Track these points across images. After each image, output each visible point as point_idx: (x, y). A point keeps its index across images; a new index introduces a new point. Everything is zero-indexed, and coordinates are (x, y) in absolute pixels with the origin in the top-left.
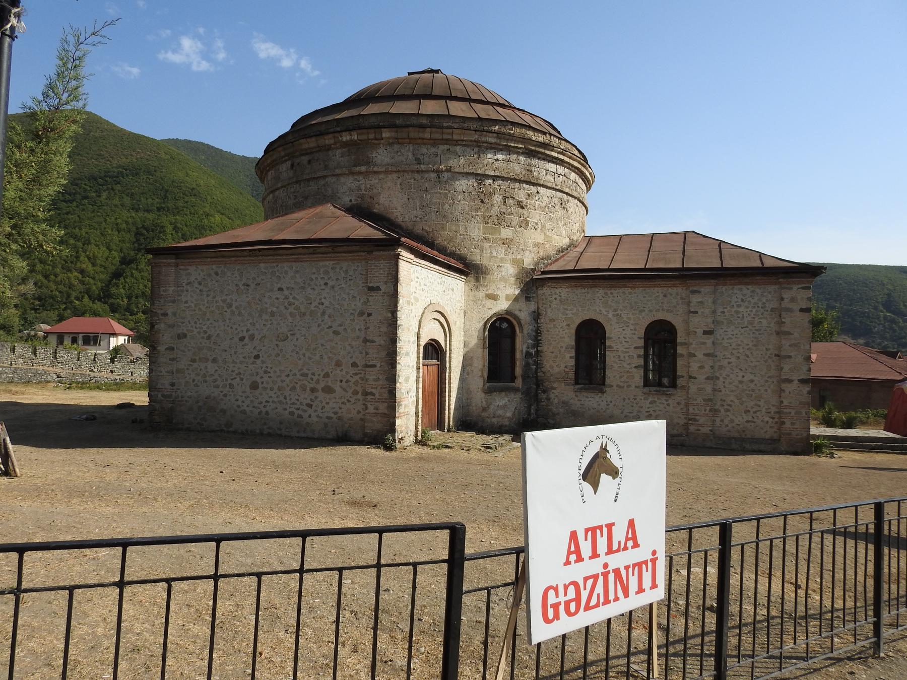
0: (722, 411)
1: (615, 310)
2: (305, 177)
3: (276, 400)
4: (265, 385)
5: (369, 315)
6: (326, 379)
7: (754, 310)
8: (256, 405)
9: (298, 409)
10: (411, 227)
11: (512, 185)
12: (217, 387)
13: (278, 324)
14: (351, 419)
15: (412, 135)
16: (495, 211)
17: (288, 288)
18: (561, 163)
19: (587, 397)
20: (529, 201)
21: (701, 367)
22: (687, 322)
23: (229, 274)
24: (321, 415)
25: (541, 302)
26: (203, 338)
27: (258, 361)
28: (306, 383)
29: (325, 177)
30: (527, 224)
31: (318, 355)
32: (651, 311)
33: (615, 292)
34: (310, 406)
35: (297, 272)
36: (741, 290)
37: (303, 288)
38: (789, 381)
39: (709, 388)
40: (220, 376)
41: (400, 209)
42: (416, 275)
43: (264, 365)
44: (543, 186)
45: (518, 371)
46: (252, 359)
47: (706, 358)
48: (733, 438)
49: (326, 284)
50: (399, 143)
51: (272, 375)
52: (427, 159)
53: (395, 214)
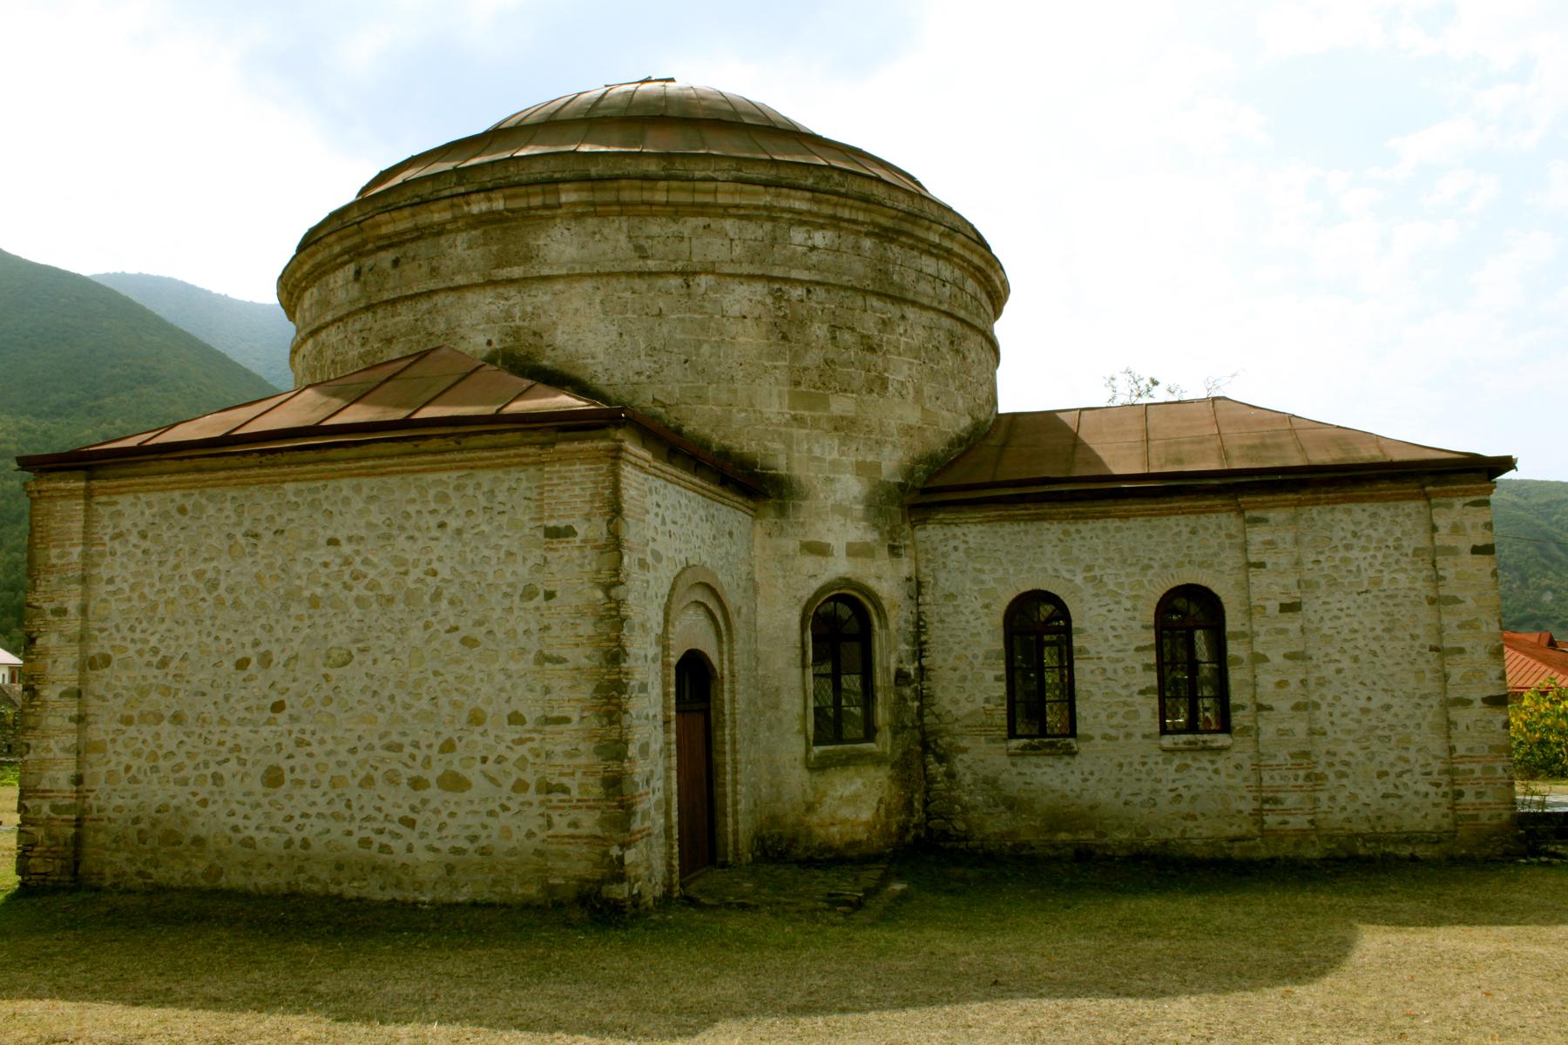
0: (1332, 777)
1: (1089, 568)
2: (386, 296)
3: (327, 812)
4: (298, 775)
5: (550, 595)
6: (447, 757)
7: (1379, 555)
8: (280, 824)
9: (381, 832)
10: (627, 398)
12: (184, 782)
13: (328, 625)
14: (512, 852)
15: (626, 196)
16: (813, 358)
17: (350, 539)
18: (947, 255)
19: (1037, 766)
21: (1282, 684)
22: (1246, 586)
23: (211, 510)
24: (437, 844)
25: (921, 556)
26: (149, 664)
27: (282, 717)
28: (399, 767)
29: (430, 293)
30: (884, 384)
31: (426, 698)
32: (1165, 566)
33: (1088, 528)
34: (409, 823)
35: (371, 499)
36: (1349, 512)
37: (388, 537)
38: (1465, 703)
39: (1300, 728)
40: (190, 755)
41: (601, 357)
42: (655, 498)
43: (296, 727)
44: (914, 303)
45: (882, 715)
46: (268, 714)
47: (1289, 663)
48: (1357, 835)
49: (442, 525)
50: (596, 214)
51: (315, 748)
52: (660, 247)
53: (590, 370)
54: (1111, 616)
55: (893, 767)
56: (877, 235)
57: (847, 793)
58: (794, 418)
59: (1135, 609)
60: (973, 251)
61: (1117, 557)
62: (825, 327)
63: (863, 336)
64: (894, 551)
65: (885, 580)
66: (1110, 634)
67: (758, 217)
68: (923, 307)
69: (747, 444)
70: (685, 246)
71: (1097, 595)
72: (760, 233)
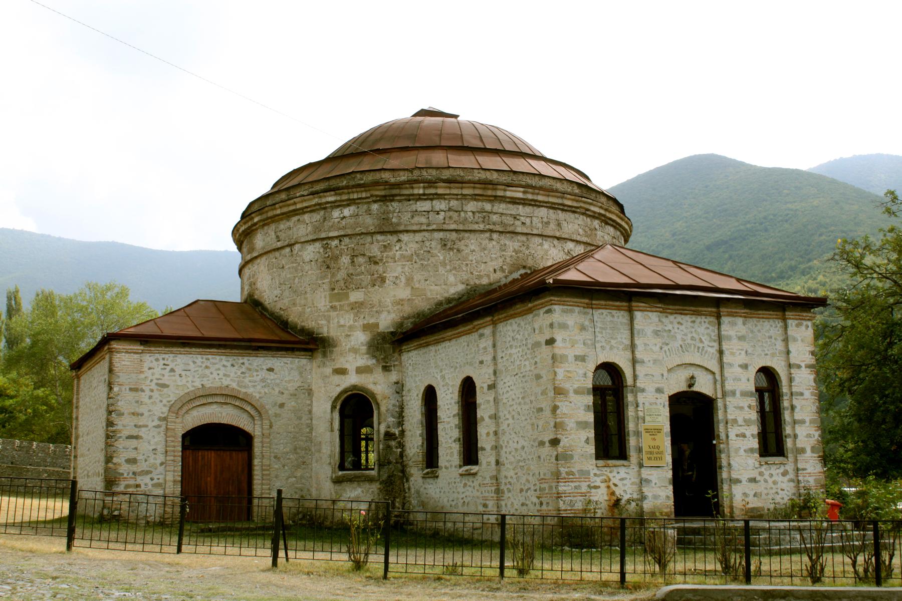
11: (361, 241)
16: (341, 275)
20: (385, 255)
30: (383, 280)
42: (162, 362)
44: (407, 231)
55: (381, 484)
56: (379, 201)
58: (332, 307)
63: (370, 258)
64: (386, 369)
65: (378, 385)
67: (317, 210)
68: (415, 231)
69: (310, 324)
72: (319, 217)
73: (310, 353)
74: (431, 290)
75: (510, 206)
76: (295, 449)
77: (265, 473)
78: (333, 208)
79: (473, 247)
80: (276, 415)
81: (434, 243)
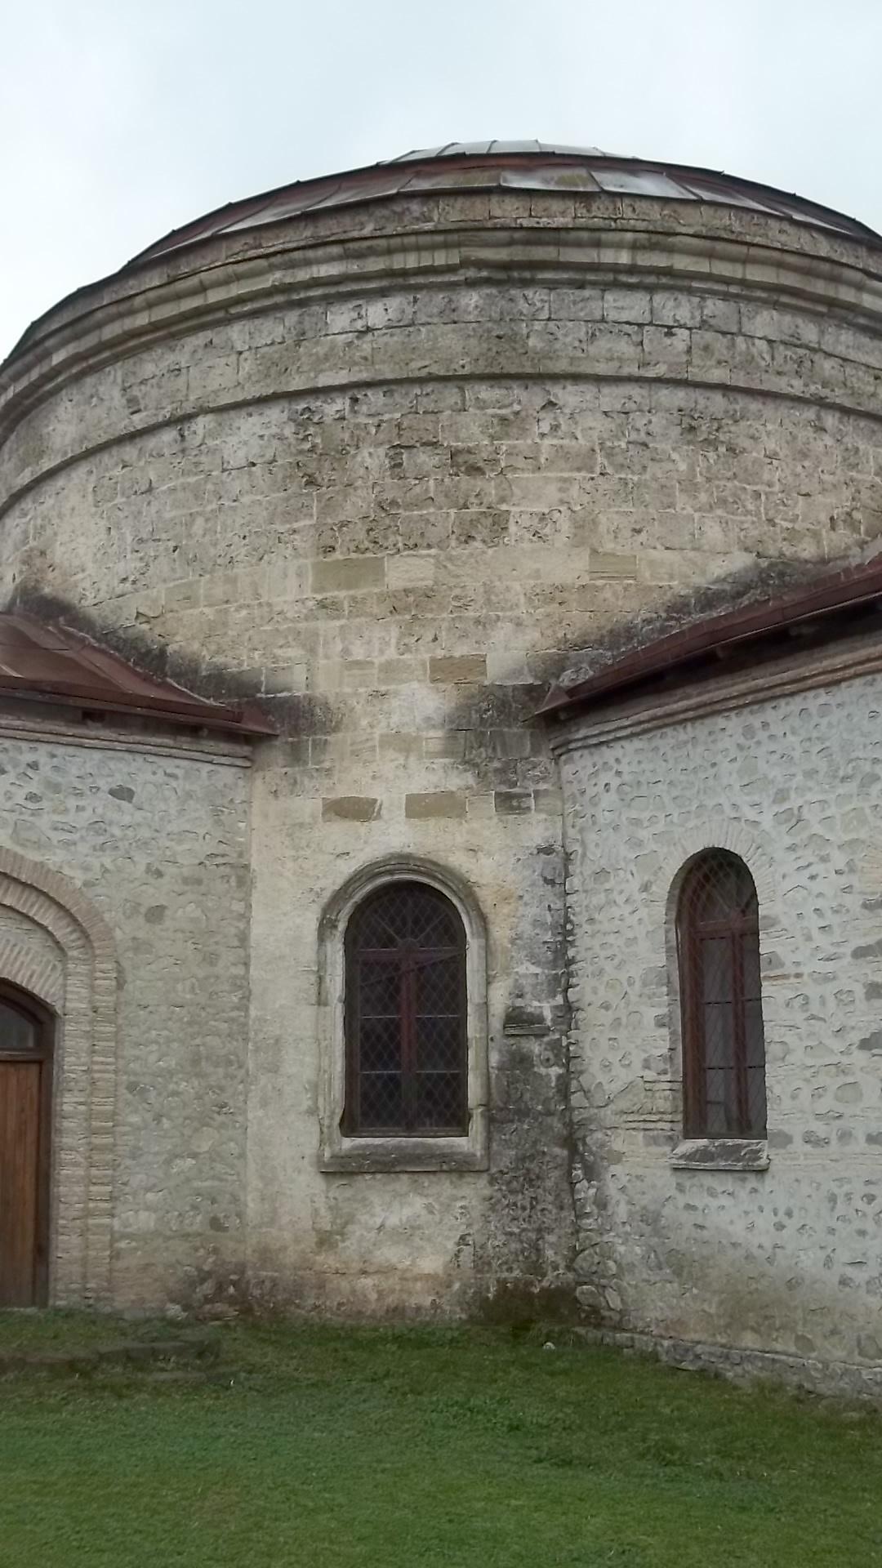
11: (427, 404)
16: (358, 504)
19: (712, 1193)
20: (505, 445)
30: (499, 524)
41: (91, 568)
44: (576, 378)
54: (816, 887)
55: (492, 1181)
56: (488, 282)
57: (393, 1220)
59: (852, 868)
60: (745, 261)
61: (823, 766)
62: (382, 451)
64: (509, 803)
65: (486, 854)
66: (815, 922)
67: (276, 308)
68: (600, 380)
69: (243, 654)
70: (181, 382)
71: (792, 848)
72: (279, 331)
73: (246, 750)
74: (652, 563)
75: (865, 340)
76: (196, 1061)
77: (97, 1140)
78: (329, 300)
79: (771, 445)
80: (138, 946)
81: (658, 422)
